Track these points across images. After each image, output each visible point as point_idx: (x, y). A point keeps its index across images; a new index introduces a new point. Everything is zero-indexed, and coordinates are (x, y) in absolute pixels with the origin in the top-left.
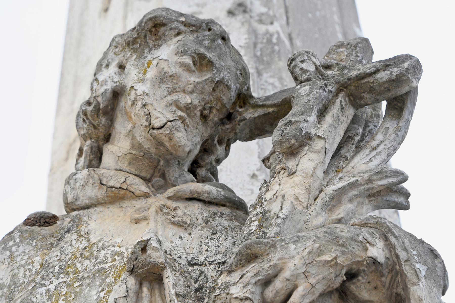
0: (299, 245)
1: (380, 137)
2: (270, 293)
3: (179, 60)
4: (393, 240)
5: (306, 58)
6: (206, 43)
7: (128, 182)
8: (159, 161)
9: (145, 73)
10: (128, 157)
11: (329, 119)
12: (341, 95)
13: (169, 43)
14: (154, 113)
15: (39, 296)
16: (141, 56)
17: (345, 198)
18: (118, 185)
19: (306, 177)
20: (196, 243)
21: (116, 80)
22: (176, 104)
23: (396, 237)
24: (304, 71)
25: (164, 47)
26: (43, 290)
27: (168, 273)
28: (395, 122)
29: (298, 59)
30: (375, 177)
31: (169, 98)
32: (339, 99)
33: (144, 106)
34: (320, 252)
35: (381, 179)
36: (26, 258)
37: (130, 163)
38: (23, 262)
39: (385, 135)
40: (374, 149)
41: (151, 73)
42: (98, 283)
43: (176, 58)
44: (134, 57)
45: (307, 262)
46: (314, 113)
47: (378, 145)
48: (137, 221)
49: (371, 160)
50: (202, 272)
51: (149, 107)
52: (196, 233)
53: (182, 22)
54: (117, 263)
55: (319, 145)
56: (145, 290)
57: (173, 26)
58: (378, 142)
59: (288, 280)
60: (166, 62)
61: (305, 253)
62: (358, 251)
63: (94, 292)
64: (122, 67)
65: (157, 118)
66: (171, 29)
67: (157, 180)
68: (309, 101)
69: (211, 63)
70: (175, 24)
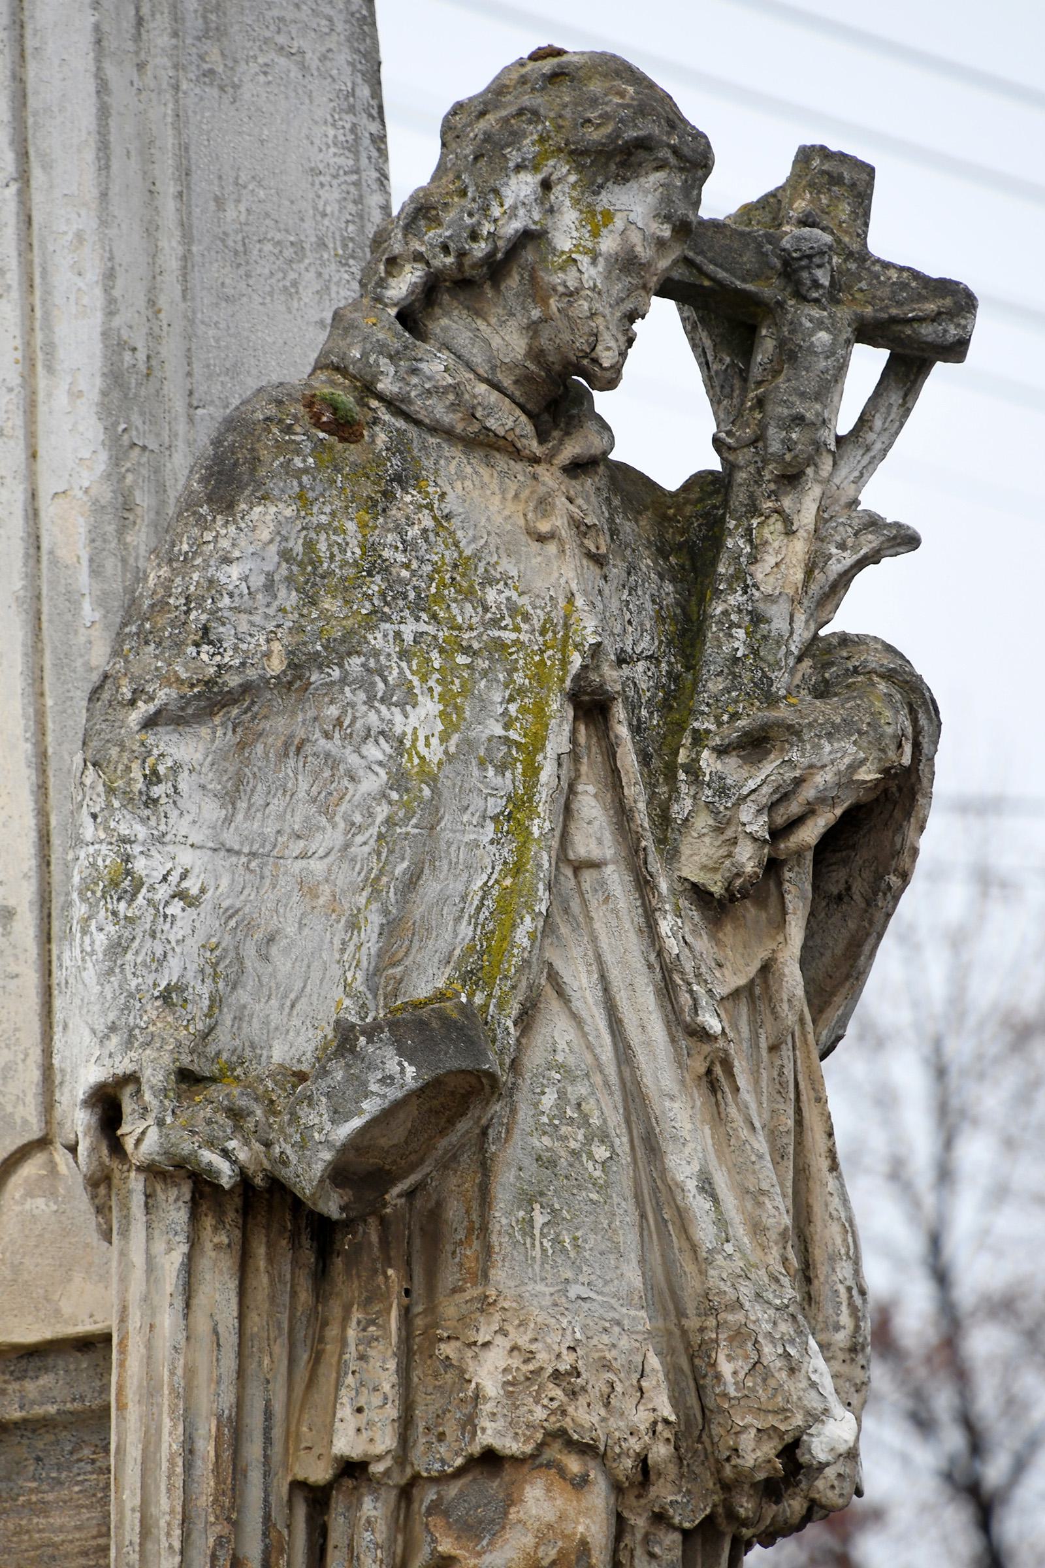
9: (595, 234)
10: (518, 371)
15: (379, 636)
18: (501, 432)
37: (516, 382)
38: (324, 519)
44: (573, 178)
51: (600, 321)
57: (660, 155)
63: (497, 697)
64: (546, 185)
65: (608, 349)
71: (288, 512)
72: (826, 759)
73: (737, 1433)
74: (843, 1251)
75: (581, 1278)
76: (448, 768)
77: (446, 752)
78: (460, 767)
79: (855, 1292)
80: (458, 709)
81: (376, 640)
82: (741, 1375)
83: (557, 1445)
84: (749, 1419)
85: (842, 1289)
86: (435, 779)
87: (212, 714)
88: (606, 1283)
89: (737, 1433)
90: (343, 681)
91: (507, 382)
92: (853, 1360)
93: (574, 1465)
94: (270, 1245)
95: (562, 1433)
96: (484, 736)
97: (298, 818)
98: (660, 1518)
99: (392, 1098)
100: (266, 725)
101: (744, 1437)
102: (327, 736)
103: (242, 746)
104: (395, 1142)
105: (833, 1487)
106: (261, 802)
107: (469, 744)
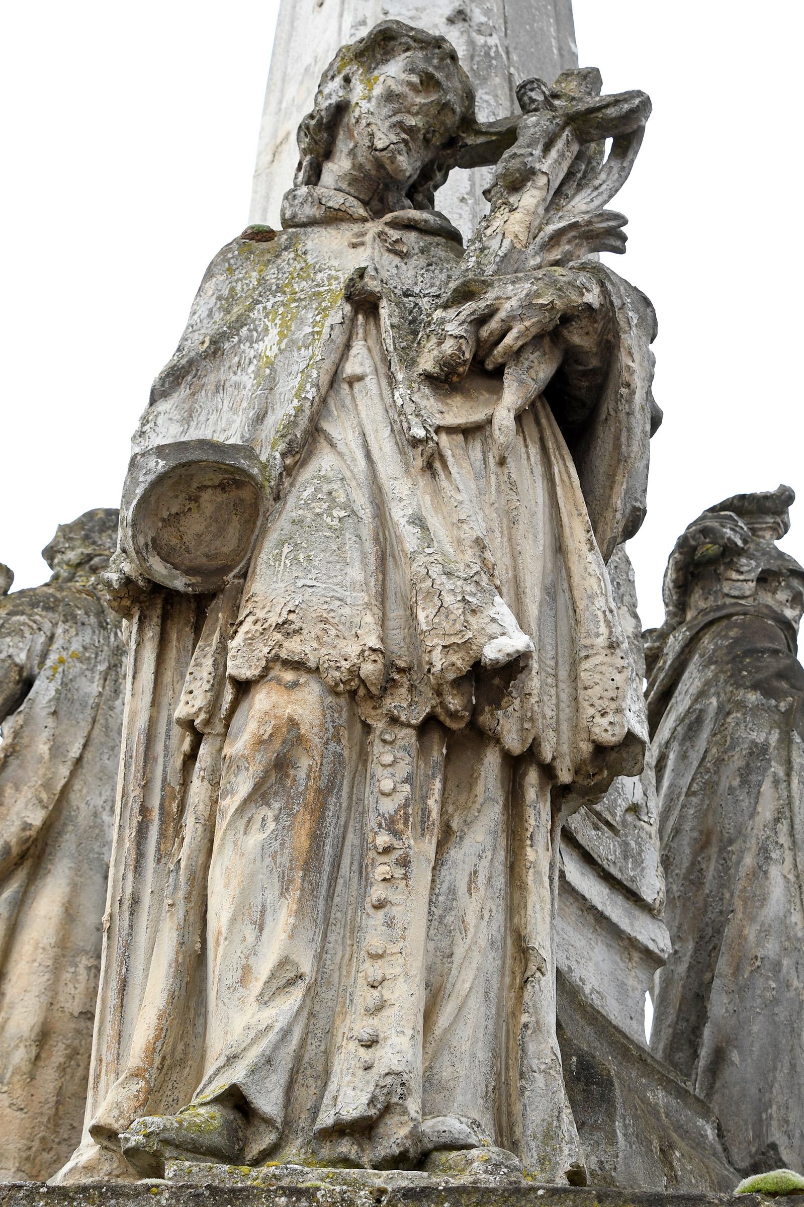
0: (517, 286)
1: (603, 176)
2: (485, 332)
3: (407, 79)
4: (609, 287)
5: (536, 86)
6: (435, 61)
7: (347, 204)
8: (379, 184)
11: (554, 154)
13: (397, 58)
14: (378, 135)
16: (369, 70)
17: (565, 239)
18: (337, 207)
19: (528, 214)
20: (411, 273)
21: (340, 94)
22: (400, 125)
23: (613, 284)
24: (533, 101)
25: (392, 62)
26: (260, 306)
27: (384, 303)
28: (620, 162)
29: (529, 87)
30: (595, 220)
31: (395, 119)
33: (368, 125)
34: (538, 295)
35: (602, 221)
36: (244, 271)
37: (349, 184)
38: (241, 276)
39: (609, 174)
40: (596, 188)
41: (378, 90)
42: (314, 306)
43: (404, 76)
44: (360, 72)
45: (524, 304)
46: (540, 147)
47: (601, 185)
48: (354, 246)
49: (592, 200)
50: (417, 304)
51: (373, 127)
52: (413, 262)
53: (412, 37)
54: (333, 287)
55: (542, 181)
56: (360, 317)
57: (403, 41)
59: (503, 321)
60: (393, 80)
61: (522, 296)
62: (574, 296)
63: (310, 315)
64: (347, 80)
65: (380, 139)
66: (400, 44)
67: (375, 203)
68: (536, 133)
69: (438, 84)
70: (404, 40)
71: (222, 278)
72: (510, 294)
73: (430, 652)
74: (598, 592)
75: (310, 576)
76: (280, 357)
77: (279, 349)
78: (287, 354)
79: (607, 613)
80: (288, 328)
81: (254, 315)
83: (278, 666)
84: (436, 641)
85: (600, 614)
86: (272, 364)
87: (179, 384)
88: (330, 578)
89: (430, 652)
90: (240, 342)
91: (344, 186)
92: (612, 653)
93: (289, 676)
94: (179, 632)
95: (277, 658)
96: (302, 336)
97: (224, 421)
98: (394, 721)
99: (149, 481)
100: (205, 380)
101: (434, 653)
102: (235, 373)
104: (232, 548)
105: (606, 730)
106: (205, 419)
107: (293, 341)
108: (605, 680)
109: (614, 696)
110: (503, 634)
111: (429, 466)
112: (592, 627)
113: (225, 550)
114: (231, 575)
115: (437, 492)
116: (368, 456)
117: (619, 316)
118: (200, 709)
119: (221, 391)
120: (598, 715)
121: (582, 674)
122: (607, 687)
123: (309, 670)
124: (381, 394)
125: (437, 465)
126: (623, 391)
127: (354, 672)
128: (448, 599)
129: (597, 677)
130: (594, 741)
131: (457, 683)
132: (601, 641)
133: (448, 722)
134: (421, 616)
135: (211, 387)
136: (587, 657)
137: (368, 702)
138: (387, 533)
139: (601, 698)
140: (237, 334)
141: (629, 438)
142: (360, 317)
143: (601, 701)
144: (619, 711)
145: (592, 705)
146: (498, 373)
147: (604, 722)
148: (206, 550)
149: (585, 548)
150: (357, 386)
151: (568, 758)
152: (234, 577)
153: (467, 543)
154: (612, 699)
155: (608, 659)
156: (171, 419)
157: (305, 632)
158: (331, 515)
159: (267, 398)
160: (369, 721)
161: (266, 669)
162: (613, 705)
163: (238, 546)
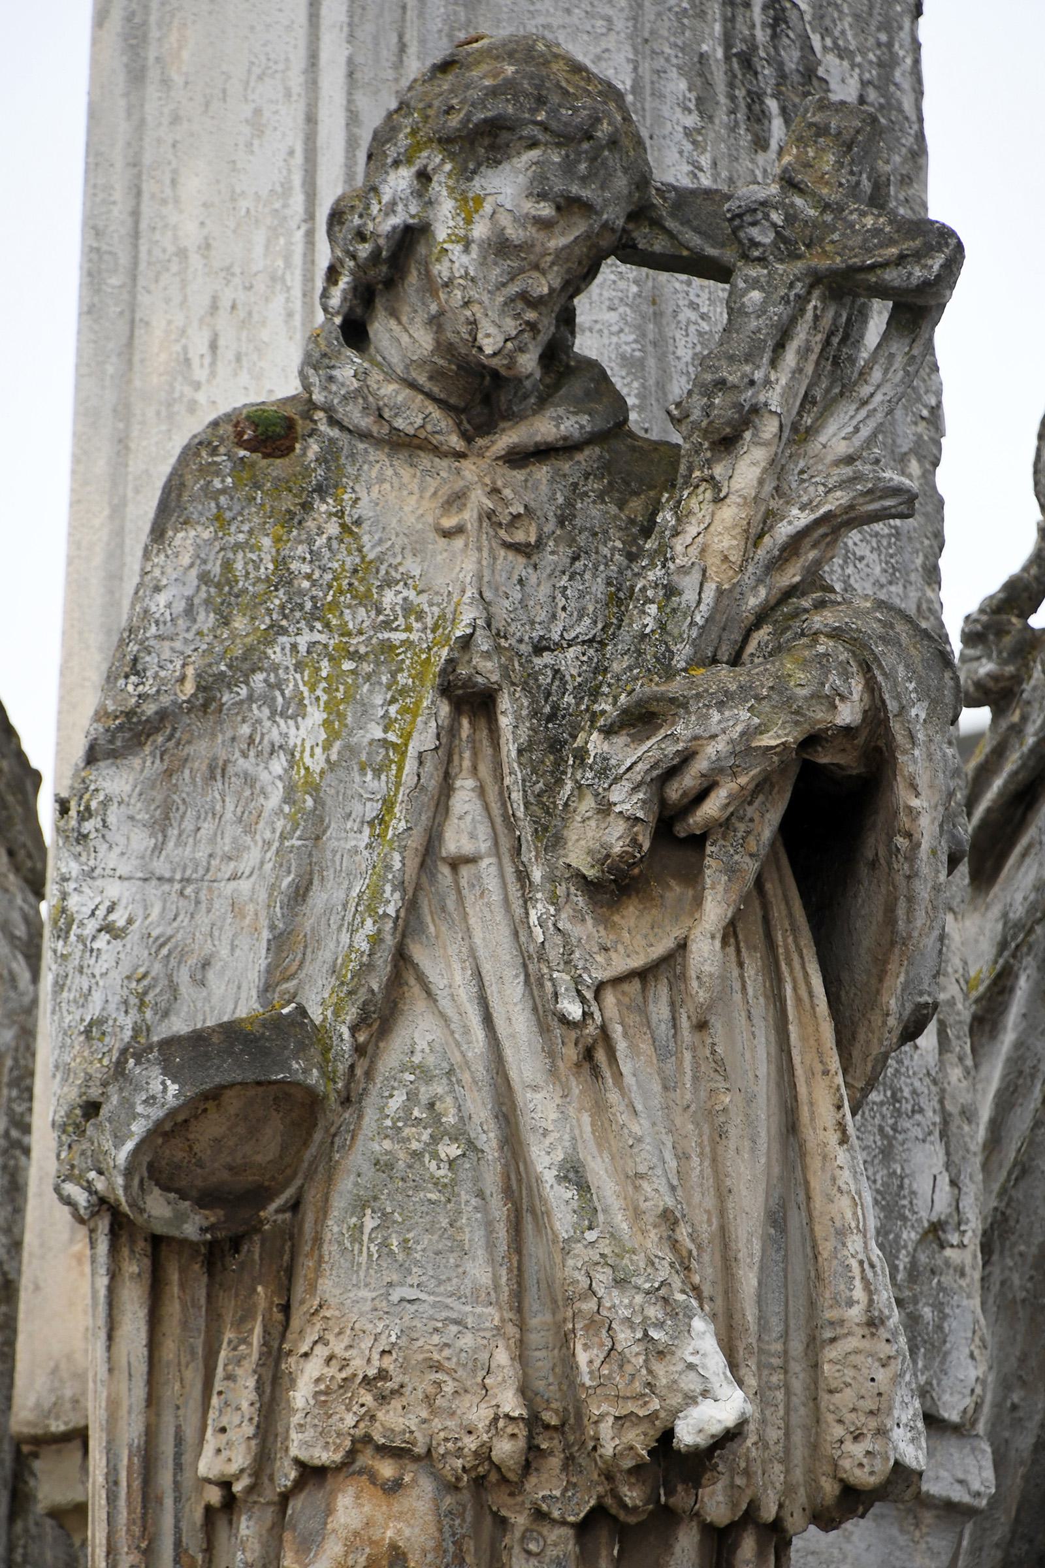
10: (428, 368)
12: (816, 293)
15: (278, 649)
18: (412, 432)
30: (861, 500)
32: (813, 303)
35: (872, 501)
39: (886, 371)
40: (864, 403)
44: (448, 167)
47: (872, 395)
51: (476, 308)
54: (414, 636)
56: (465, 722)
58: (871, 389)
59: (703, 776)
73: (596, 1422)
74: (853, 1225)
77: (328, 761)
78: (341, 773)
79: (866, 1266)
82: (597, 1363)
85: (854, 1264)
89: (596, 1422)
90: (251, 698)
93: (387, 1469)
95: (367, 1439)
100: (189, 750)
101: (602, 1425)
102: (245, 755)
103: (169, 773)
104: (270, 1157)
105: (861, 1465)
108: (861, 1379)
109: (874, 1407)
110: (705, 1393)
111: (588, 1054)
112: (842, 1287)
113: (259, 1158)
114: (273, 1206)
115: (600, 1108)
116: (488, 1020)
117: (896, 727)
118: (242, 1471)
119: (219, 777)
120: (849, 1437)
121: (826, 1367)
122: (863, 1392)
123: (417, 1459)
124: (506, 901)
125: (601, 1056)
126: (901, 841)
127: (484, 1454)
128: (624, 1337)
129: (849, 1373)
130: (841, 1480)
131: (637, 1470)
132: (855, 1313)
133: (622, 1516)
134: (582, 1358)
135: (200, 766)
136: (833, 1340)
137: (503, 1488)
138: (522, 1168)
139: (854, 1410)
140: (247, 683)
141: (910, 911)
142: (465, 722)
143: (853, 1415)
144: (882, 1432)
145: (840, 1421)
146: (698, 842)
147: (857, 1450)
148: (229, 1159)
149: (833, 1138)
150: (465, 871)
151: (802, 1491)
152: (277, 1211)
153: (650, 1218)
154: (871, 1412)
155: (866, 1344)
156: (131, 818)
157: (407, 1390)
158: (435, 1156)
159: (310, 855)
160: (504, 1513)
161: (352, 1454)
162: (873, 1424)
163: (281, 1157)
